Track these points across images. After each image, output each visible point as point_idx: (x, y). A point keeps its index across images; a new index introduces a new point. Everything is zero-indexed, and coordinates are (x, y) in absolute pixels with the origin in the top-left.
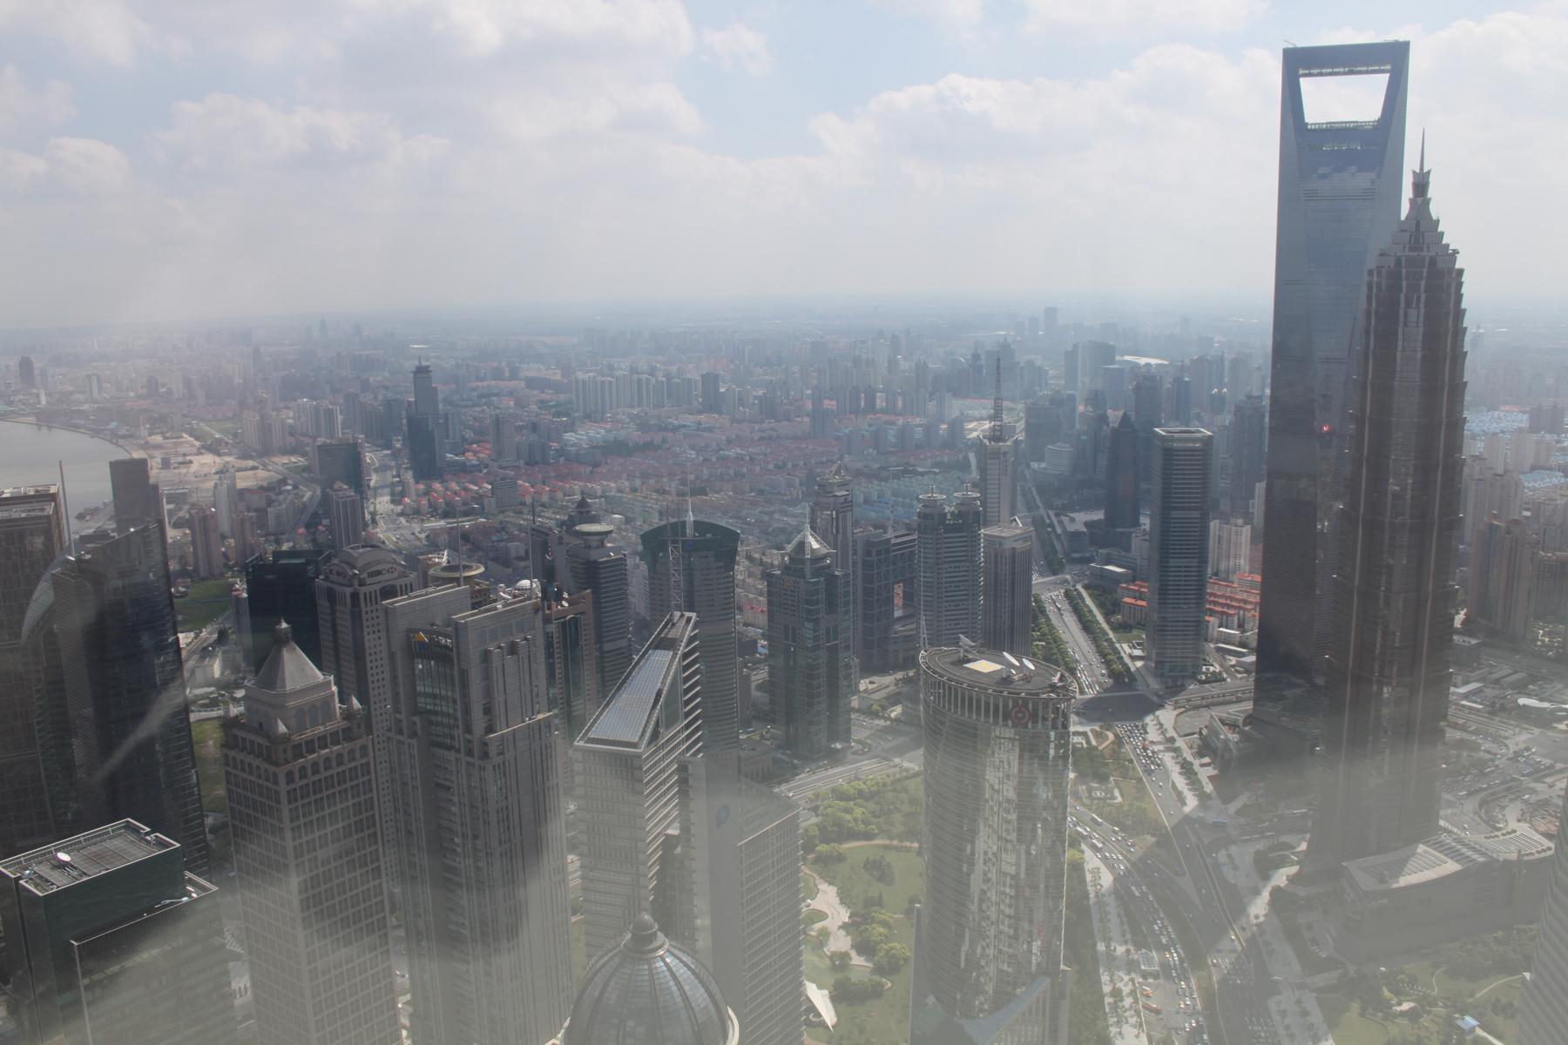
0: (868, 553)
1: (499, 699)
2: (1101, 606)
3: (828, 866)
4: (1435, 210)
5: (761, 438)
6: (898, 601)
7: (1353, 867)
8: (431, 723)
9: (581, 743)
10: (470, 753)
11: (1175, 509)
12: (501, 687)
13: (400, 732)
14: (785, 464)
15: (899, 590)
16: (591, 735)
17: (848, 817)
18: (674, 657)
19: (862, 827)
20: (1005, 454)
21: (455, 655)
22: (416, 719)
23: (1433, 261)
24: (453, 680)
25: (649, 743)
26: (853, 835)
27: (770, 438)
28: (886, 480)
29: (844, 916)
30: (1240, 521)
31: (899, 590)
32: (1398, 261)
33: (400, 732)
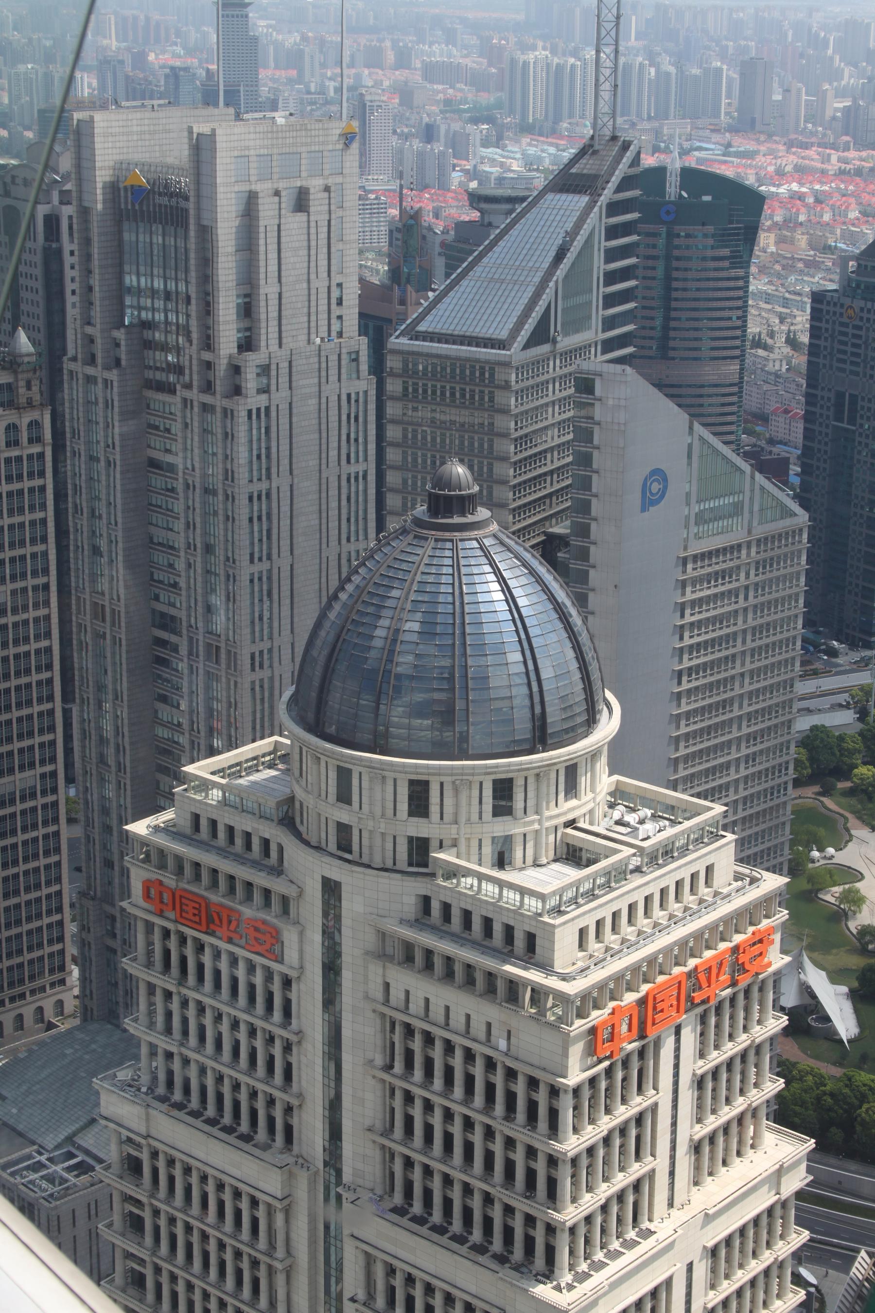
1: (268, 289)
5: (842, 172)
8: (149, 345)
9: (404, 340)
10: (208, 387)
12: (273, 268)
13: (91, 360)
16: (422, 327)
21: (191, 206)
22: (120, 335)
27: (859, 172)
33: (91, 360)
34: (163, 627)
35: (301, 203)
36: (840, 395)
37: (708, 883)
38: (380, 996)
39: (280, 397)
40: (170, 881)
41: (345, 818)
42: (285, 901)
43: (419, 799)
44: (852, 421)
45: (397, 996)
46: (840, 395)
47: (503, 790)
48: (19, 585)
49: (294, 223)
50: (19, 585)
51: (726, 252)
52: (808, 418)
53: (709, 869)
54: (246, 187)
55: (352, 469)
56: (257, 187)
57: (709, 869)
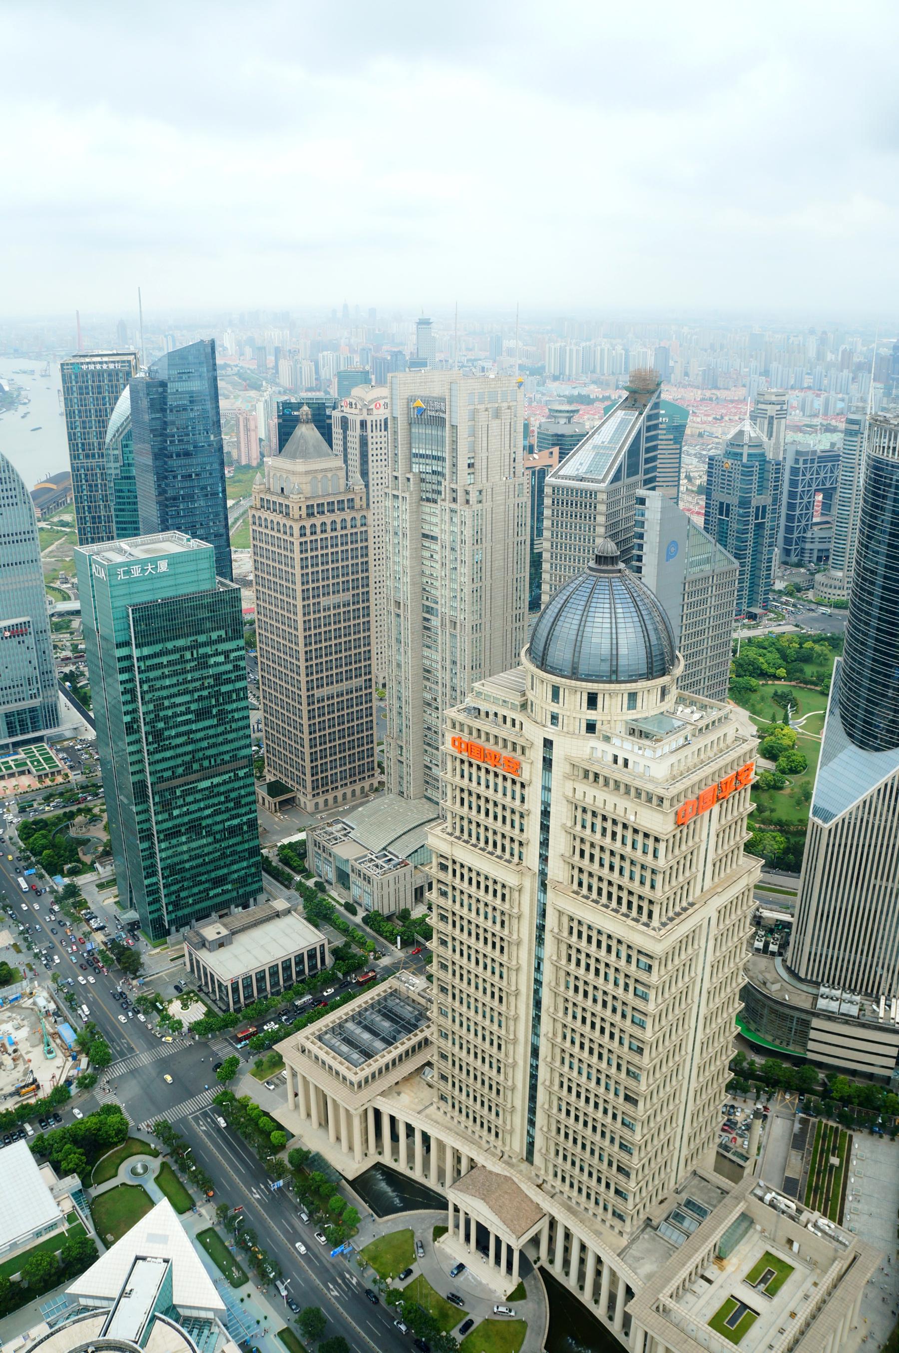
0: (797, 461)
6: (818, 508)
9: (553, 479)
12: (485, 445)
14: (722, 418)
15: (820, 497)
16: (561, 473)
17: (761, 660)
18: (641, 414)
19: (772, 671)
24: (443, 442)
25: (612, 482)
26: (763, 675)
34: (428, 612)
35: (497, 414)
36: (722, 504)
38: (570, 794)
39: (487, 505)
40: (466, 737)
41: (556, 711)
42: (523, 748)
43: (592, 700)
44: (727, 516)
45: (579, 795)
46: (722, 504)
47: (633, 696)
48: (356, 592)
49: (495, 424)
50: (356, 592)
51: (671, 437)
52: (707, 514)
54: (472, 407)
55: (519, 539)
56: (478, 407)
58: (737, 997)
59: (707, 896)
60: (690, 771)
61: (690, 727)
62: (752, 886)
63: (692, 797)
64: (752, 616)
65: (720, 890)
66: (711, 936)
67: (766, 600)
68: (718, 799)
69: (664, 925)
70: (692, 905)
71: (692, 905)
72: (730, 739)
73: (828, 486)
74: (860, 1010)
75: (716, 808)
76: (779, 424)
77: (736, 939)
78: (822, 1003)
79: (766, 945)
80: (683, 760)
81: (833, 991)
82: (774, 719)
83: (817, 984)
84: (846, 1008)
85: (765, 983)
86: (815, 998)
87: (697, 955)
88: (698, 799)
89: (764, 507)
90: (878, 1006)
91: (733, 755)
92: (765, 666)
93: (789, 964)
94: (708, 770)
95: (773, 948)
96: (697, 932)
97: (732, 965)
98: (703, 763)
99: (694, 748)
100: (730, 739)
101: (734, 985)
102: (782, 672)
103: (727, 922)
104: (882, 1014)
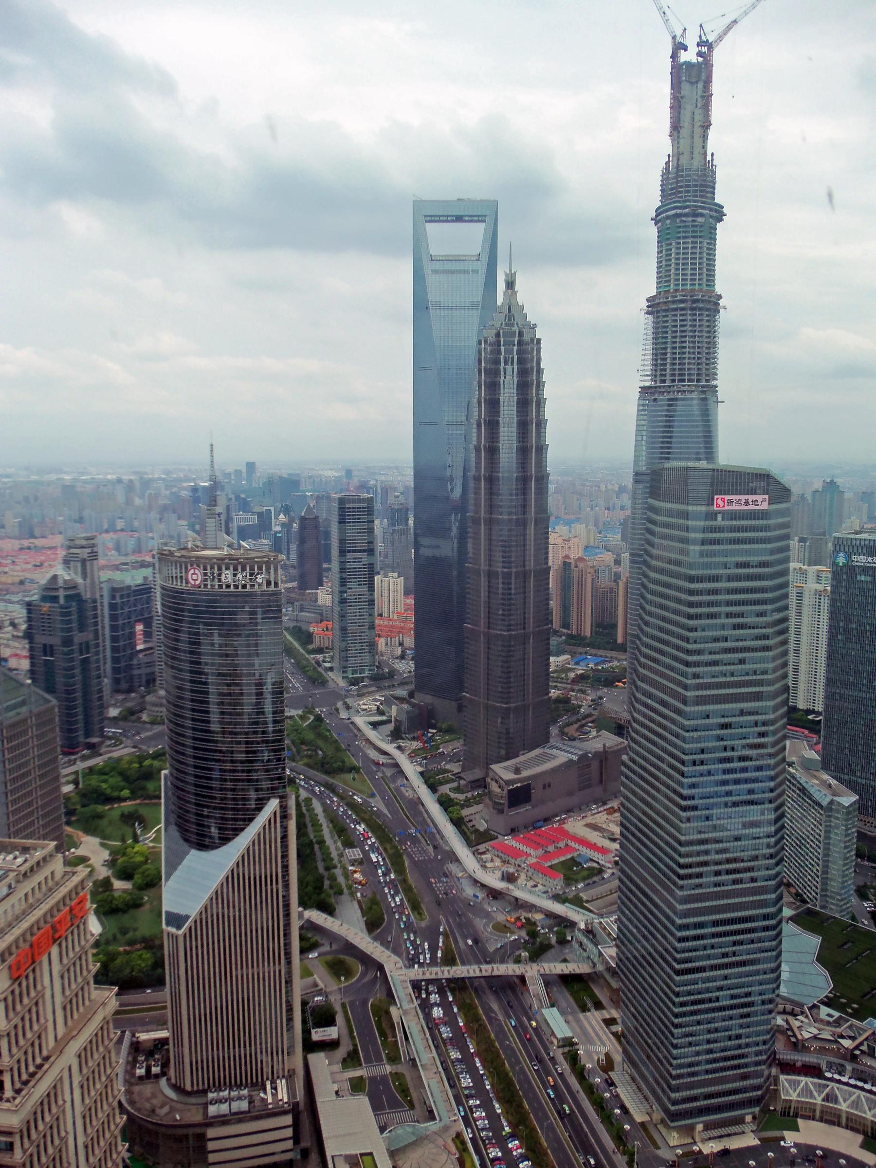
0: (113, 597)
2: (298, 639)
3: (91, 825)
4: (521, 299)
7: (495, 767)
11: (349, 551)
15: (139, 627)
17: (104, 786)
19: (116, 794)
20: (219, 515)
23: (521, 334)
28: (127, 570)
29: (106, 855)
30: (396, 575)
31: (139, 627)
32: (498, 335)
36: (45, 645)
37: (53, 878)
52: (32, 657)
53: (52, 873)
57: (52, 873)
58: (119, 1139)
59: (61, 1044)
60: (18, 919)
61: (12, 875)
62: (109, 1017)
63: (25, 946)
64: (91, 746)
65: (75, 1033)
66: (76, 1084)
67: (102, 729)
68: (55, 941)
69: (18, 1092)
70: (46, 1059)
71: (46, 1059)
72: (58, 876)
73: (146, 616)
74: (250, 1103)
75: (55, 950)
76: (92, 565)
77: (104, 1079)
78: (213, 1110)
79: (148, 1069)
80: (9, 910)
81: (221, 1094)
82: (123, 840)
83: (204, 1092)
84: (236, 1106)
85: (153, 1111)
86: (205, 1106)
87: (64, 1111)
88: (31, 946)
89: (87, 644)
90: (265, 1093)
91: (63, 891)
92: (108, 791)
93: (173, 1081)
94: (38, 913)
95: (155, 1070)
96: (59, 1086)
97: (105, 1107)
98: (32, 907)
99: (20, 894)
100: (58, 876)
101: (113, 1127)
102: (126, 793)
103: (90, 1064)
104: (270, 1100)
